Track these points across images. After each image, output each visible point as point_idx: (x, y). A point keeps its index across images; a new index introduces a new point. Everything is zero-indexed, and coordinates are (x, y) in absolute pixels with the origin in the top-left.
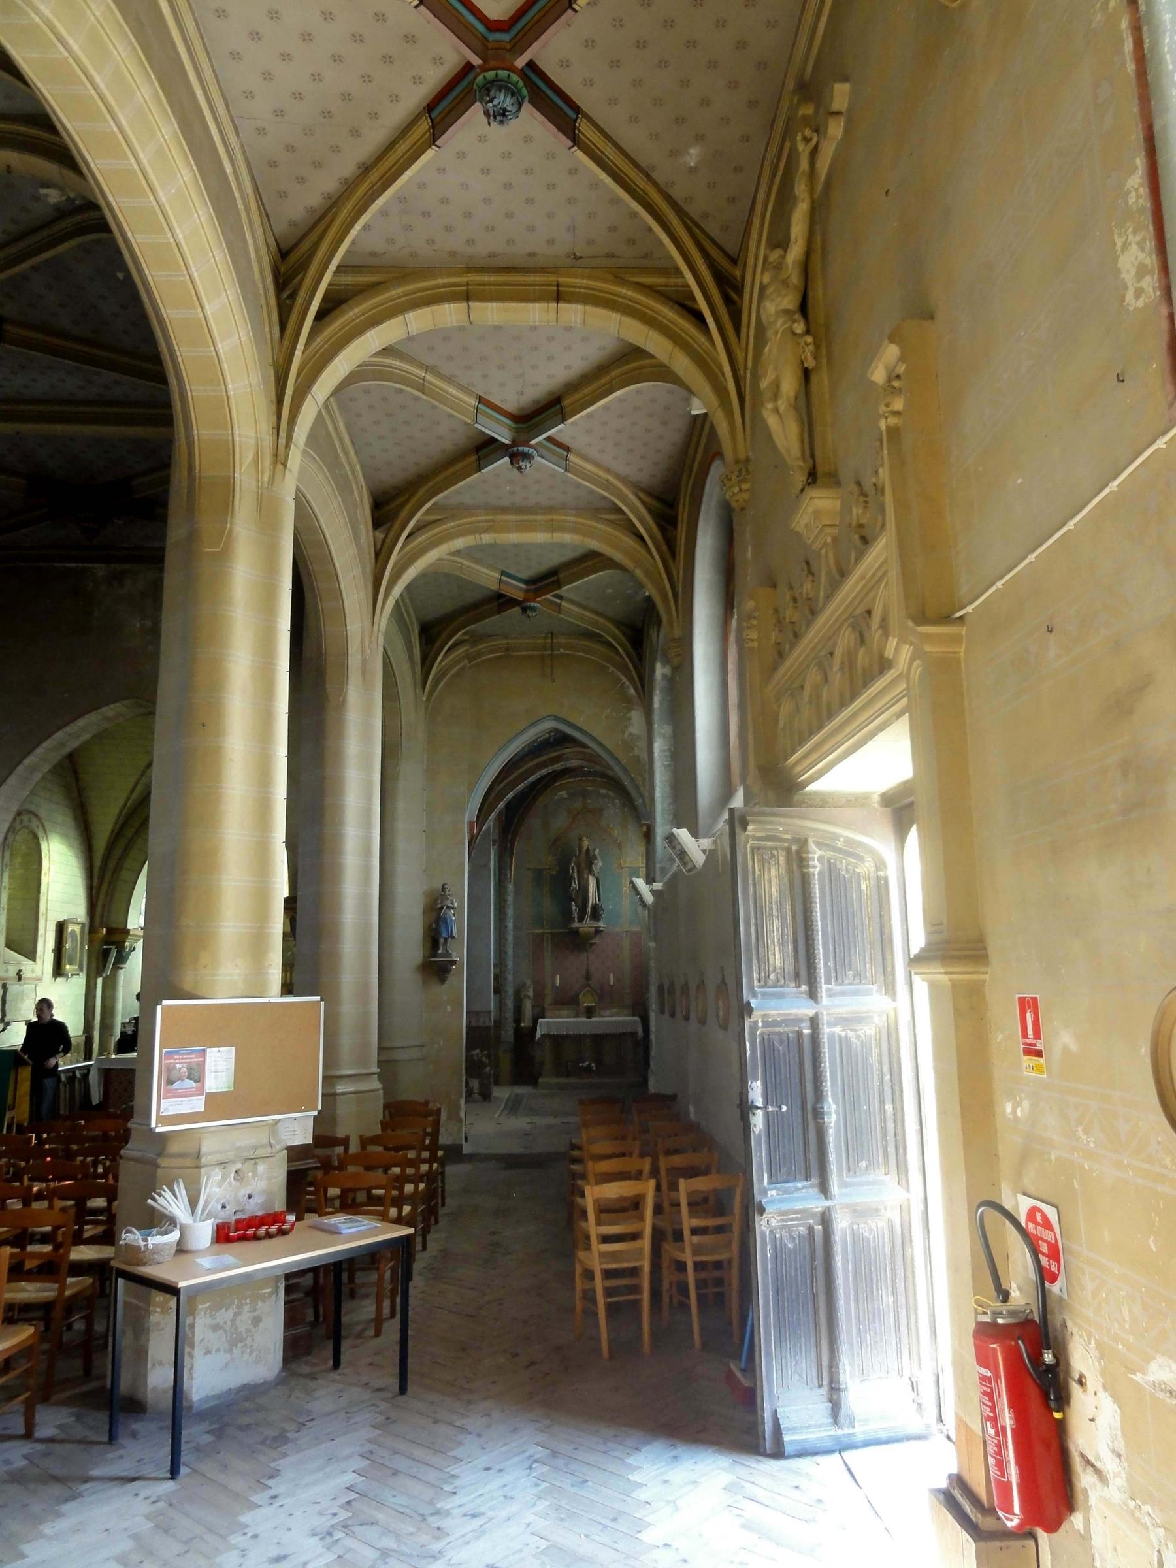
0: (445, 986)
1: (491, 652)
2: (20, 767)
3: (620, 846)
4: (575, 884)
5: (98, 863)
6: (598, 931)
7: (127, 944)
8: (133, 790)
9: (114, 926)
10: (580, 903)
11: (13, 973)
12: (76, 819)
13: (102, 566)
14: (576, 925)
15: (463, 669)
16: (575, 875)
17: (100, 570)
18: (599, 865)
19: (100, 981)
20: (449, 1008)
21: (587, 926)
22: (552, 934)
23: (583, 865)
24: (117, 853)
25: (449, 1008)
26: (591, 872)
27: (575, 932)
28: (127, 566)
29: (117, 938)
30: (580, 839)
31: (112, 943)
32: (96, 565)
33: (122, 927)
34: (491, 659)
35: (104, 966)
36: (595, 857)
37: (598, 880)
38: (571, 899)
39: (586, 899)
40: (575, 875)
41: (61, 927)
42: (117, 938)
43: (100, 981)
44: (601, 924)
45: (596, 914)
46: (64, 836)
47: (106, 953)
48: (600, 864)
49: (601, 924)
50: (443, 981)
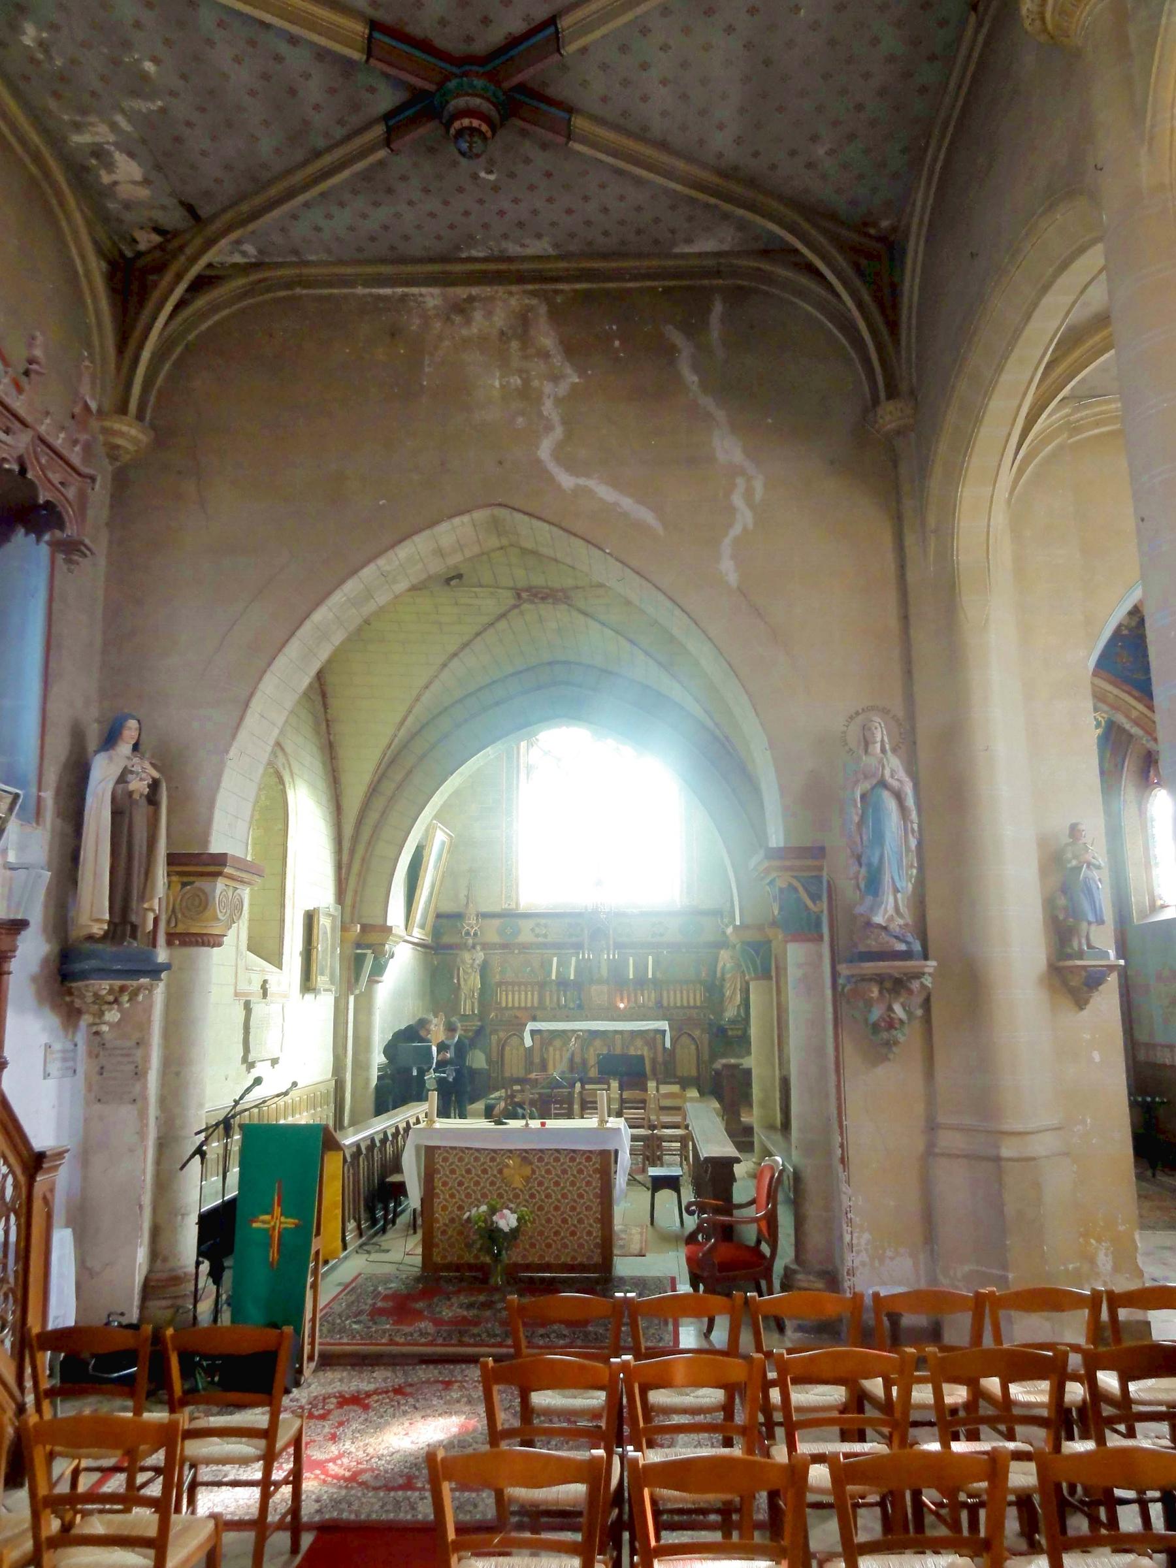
0: (1085, 1013)
1: (1098, 424)
2: (307, 626)
5: (348, 830)
7: (387, 946)
8: (402, 723)
9: (371, 922)
11: (256, 987)
12: (324, 764)
13: (436, 291)
15: (1061, 447)
17: (432, 297)
19: (352, 999)
20: (1096, 1056)
24: (373, 816)
25: (1096, 1056)
28: (475, 291)
29: (373, 938)
31: (368, 947)
32: (424, 290)
33: (380, 922)
34: (1097, 437)
35: (357, 979)
41: (310, 919)
42: (373, 938)
43: (352, 999)
46: (312, 785)
47: (359, 960)
50: (1081, 1003)
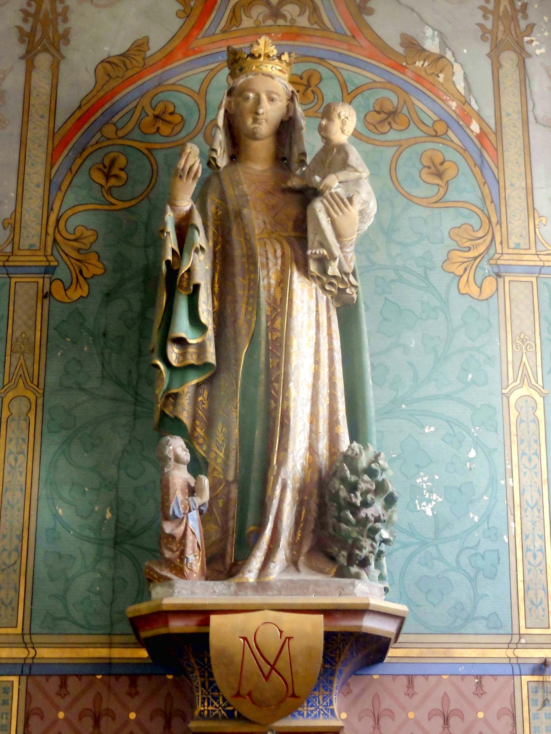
3: (488, 143)
4: (193, 332)
6: (353, 649)
10: (224, 450)
14: (190, 590)
16: (200, 266)
18: (355, 208)
21: (266, 606)
22: (26, 669)
23: (256, 220)
26: (298, 237)
27: (179, 653)
30: (237, 62)
36: (333, 157)
37: (348, 315)
38: (169, 424)
39: (268, 426)
40: (200, 266)
44: (365, 590)
45: (335, 526)
48: (366, 197)
49: (365, 590)
